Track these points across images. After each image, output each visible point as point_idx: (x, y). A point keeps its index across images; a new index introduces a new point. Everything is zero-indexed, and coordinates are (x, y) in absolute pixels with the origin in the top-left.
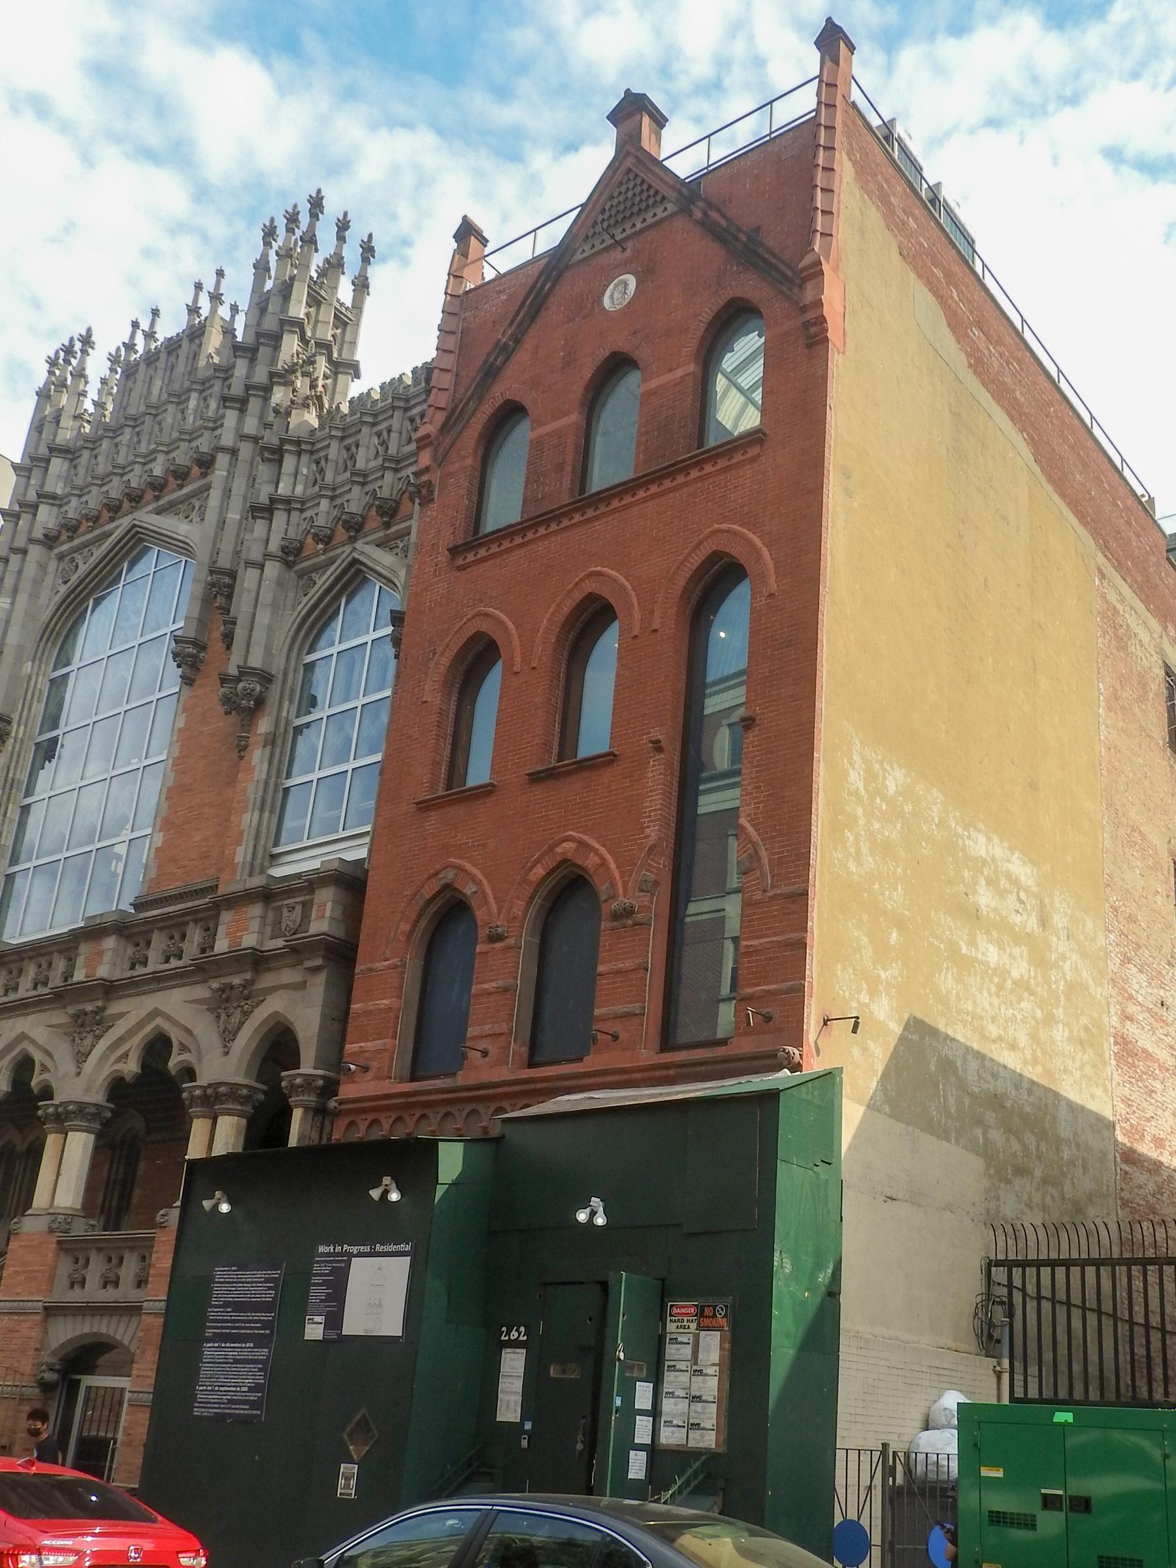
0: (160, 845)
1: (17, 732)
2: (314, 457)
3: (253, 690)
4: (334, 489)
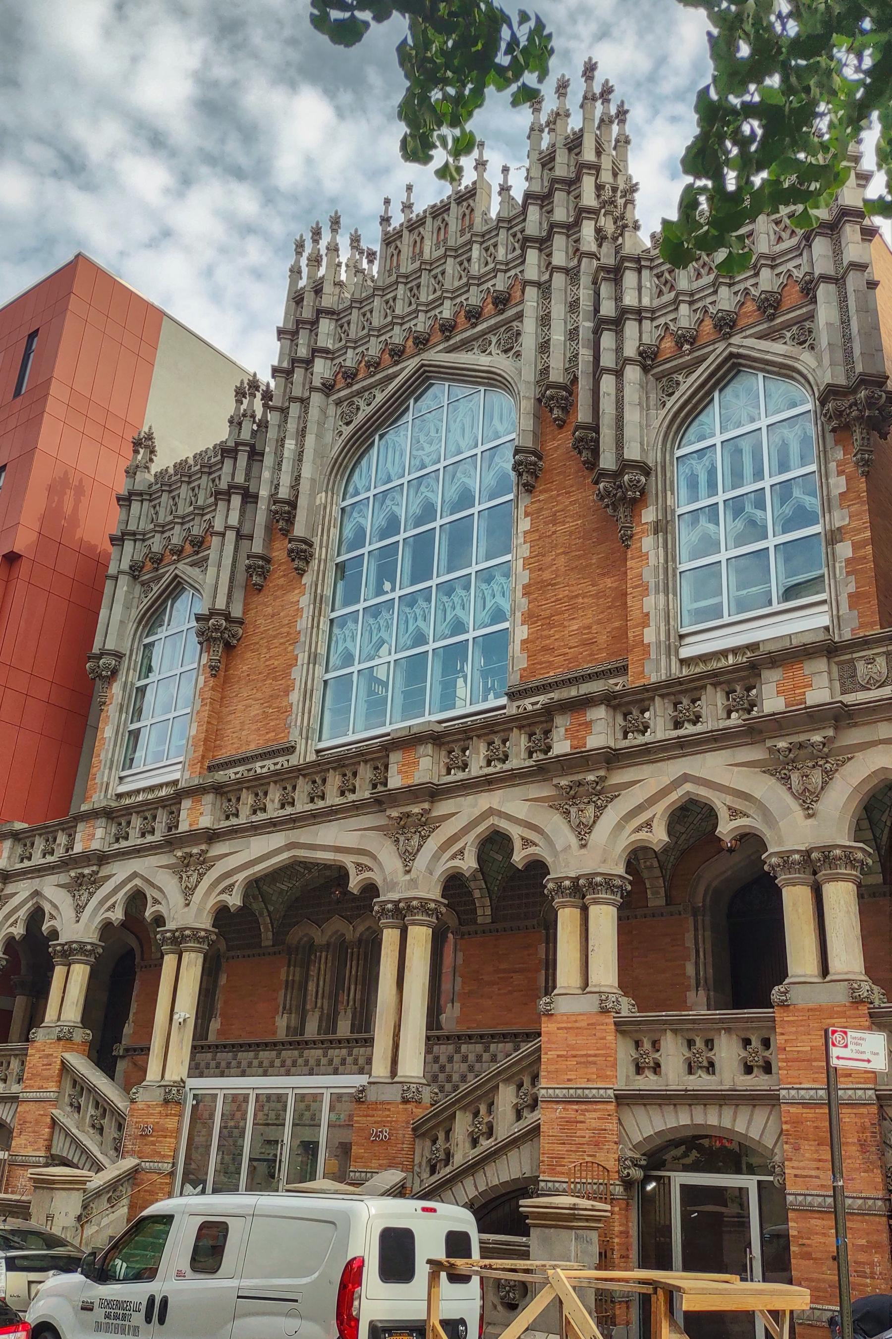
0: (525, 637)
1: (320, 555)
2: (655, 272)
3: (638, 482)
4: (692, 295)
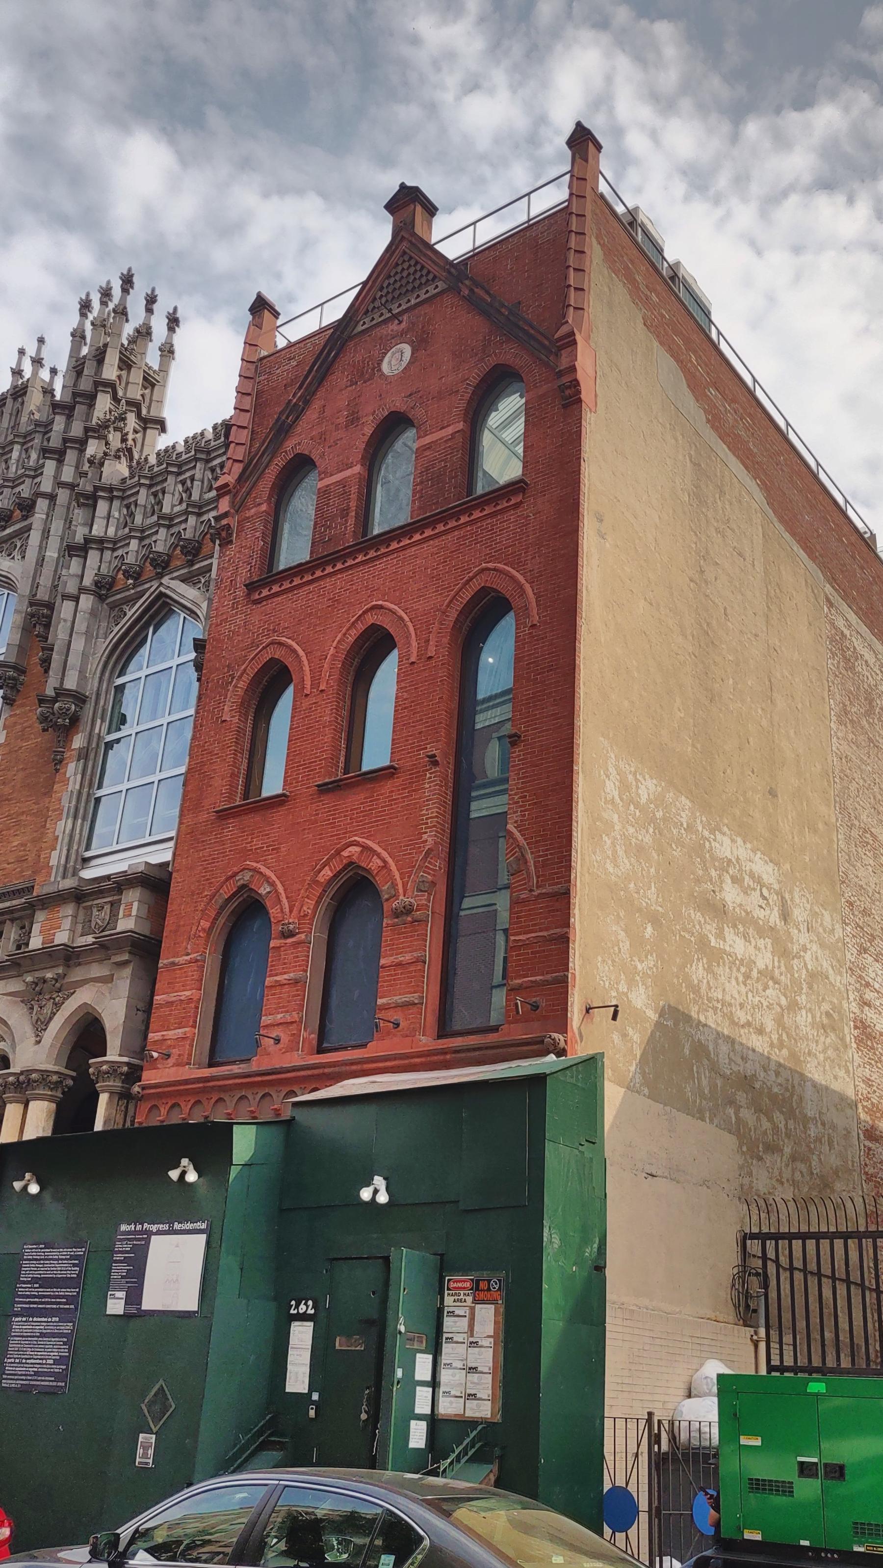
2: (125, 503)
3: (68, 710)
4: (143, 531)
